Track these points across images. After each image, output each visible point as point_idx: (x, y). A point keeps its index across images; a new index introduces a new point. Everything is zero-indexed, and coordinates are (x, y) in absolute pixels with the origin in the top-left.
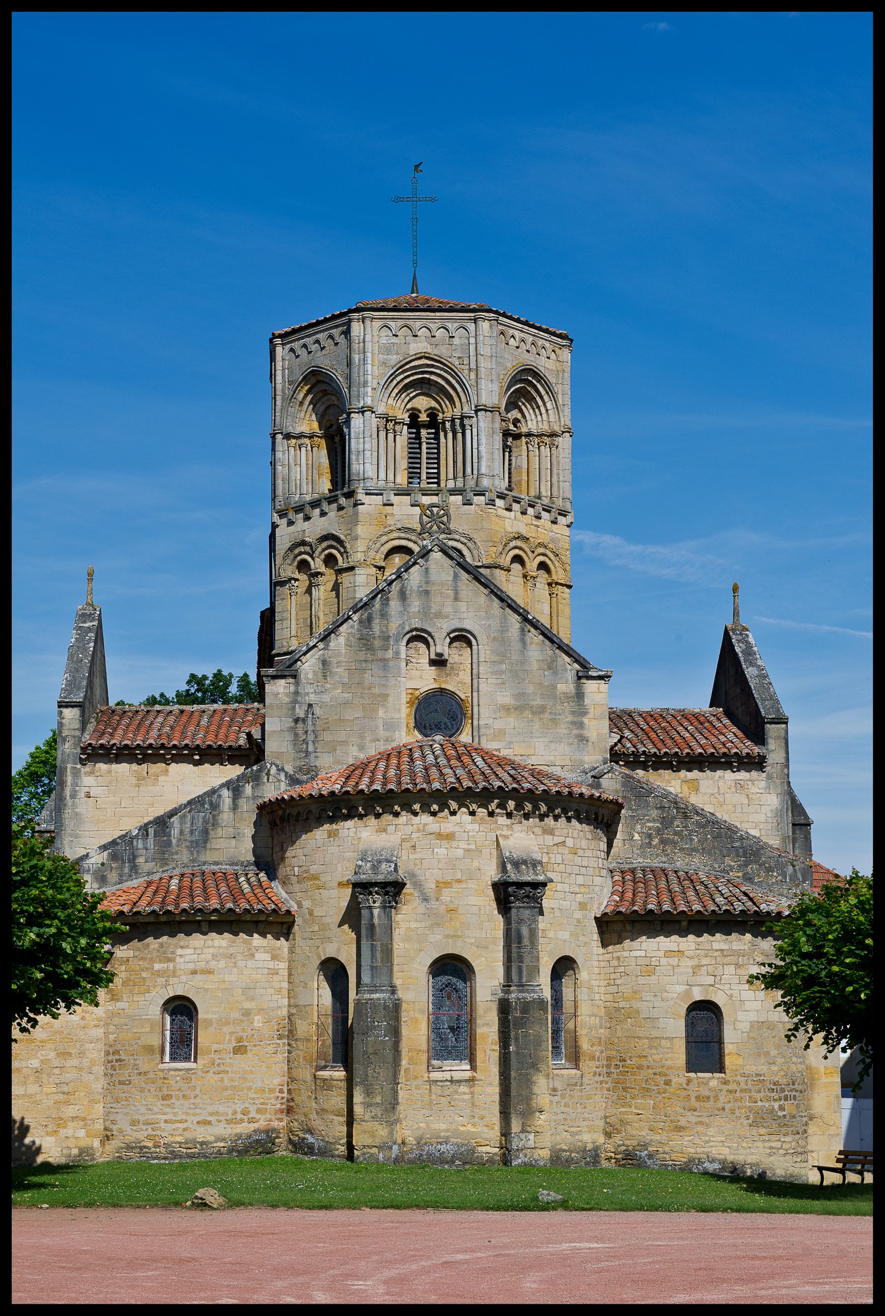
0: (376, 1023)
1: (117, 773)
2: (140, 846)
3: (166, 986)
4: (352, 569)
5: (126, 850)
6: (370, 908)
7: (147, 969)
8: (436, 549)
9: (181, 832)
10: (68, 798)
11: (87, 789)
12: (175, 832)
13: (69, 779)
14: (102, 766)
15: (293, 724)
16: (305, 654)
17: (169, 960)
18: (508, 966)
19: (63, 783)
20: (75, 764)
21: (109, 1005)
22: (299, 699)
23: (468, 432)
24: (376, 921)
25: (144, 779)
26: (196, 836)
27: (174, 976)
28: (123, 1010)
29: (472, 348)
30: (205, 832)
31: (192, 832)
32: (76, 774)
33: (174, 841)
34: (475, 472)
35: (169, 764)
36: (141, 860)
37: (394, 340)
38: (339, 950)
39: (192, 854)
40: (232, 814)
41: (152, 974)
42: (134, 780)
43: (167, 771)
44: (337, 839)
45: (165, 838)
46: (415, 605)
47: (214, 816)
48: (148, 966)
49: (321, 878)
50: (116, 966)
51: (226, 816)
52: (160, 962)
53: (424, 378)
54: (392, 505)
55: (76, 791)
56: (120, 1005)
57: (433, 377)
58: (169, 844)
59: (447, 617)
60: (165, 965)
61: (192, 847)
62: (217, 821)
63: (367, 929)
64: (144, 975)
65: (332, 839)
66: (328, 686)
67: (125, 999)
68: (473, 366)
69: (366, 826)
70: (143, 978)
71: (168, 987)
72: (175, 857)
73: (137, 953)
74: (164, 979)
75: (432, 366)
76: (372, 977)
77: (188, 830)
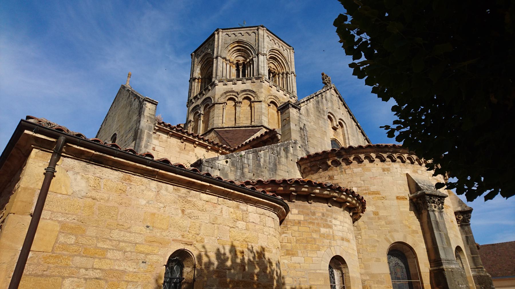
0: (460, 286)
1: (170, 143)
2: (246, 162)
3: (330, 246)
4: (261, 102)
5: (238, 161)
6: (433, 211)
7: (315, 231)
8: (333, 88)
9: (265, 161)
10: (143, 147)
11: (154, 146)
12: (262, 160)
13: (145, 137)
14: (164, 136)
15: (300, 130)
16: (302, 103)
17: (330, 227)
18: (473, 258)
19: (142, 138)
20: (150, 131)
21: (285, 259)
22: (301, 120)
23: (288, 78)
24: (438, 220)
25: (183, 150)
26: (271, 166)
27: (334, 240)
28: (299, 264)
29: (289, 56)
30: (275, 165)
31: (269, 163)
32: (149, 136)
33: (262, 164)
34: (291, 90)
35: (195, 147)
36: (246, 170)
37: (270, 41)
38: (405, 237)
39: (270, 175)
40: (286, 160)
41: (320, 236)
42: (178, 150)
43: (194, 150)
44: (389, 172)
45: (258, 162)
46: (330, 104)
47: (278, 158)
48: (316, 229)
49: (381, 194)
50: (289, 226)
51: (283, 160)
52: (324, 227)
53: (275, 58)
54: (272, 87)
55: (148, 145)
56: (295, 259)
57: (278, 59)
58: (259, 165)
59: (338, 113)
60: (328, 230)
61: (270, 171)
62: (280, 161)
63: (435, 223)
64: (315, 236)
65: (386, 172)
66: (309, 120)
67: (300, 254)
68: (290, 61)
69: (407, 168)
70: (314, 239)
71: (332, 248)
72: (262, 174)
73: (307, 218)
74: (328, 241)
75: (279, 55)
76: (445, 254)
77: (268, 161)
